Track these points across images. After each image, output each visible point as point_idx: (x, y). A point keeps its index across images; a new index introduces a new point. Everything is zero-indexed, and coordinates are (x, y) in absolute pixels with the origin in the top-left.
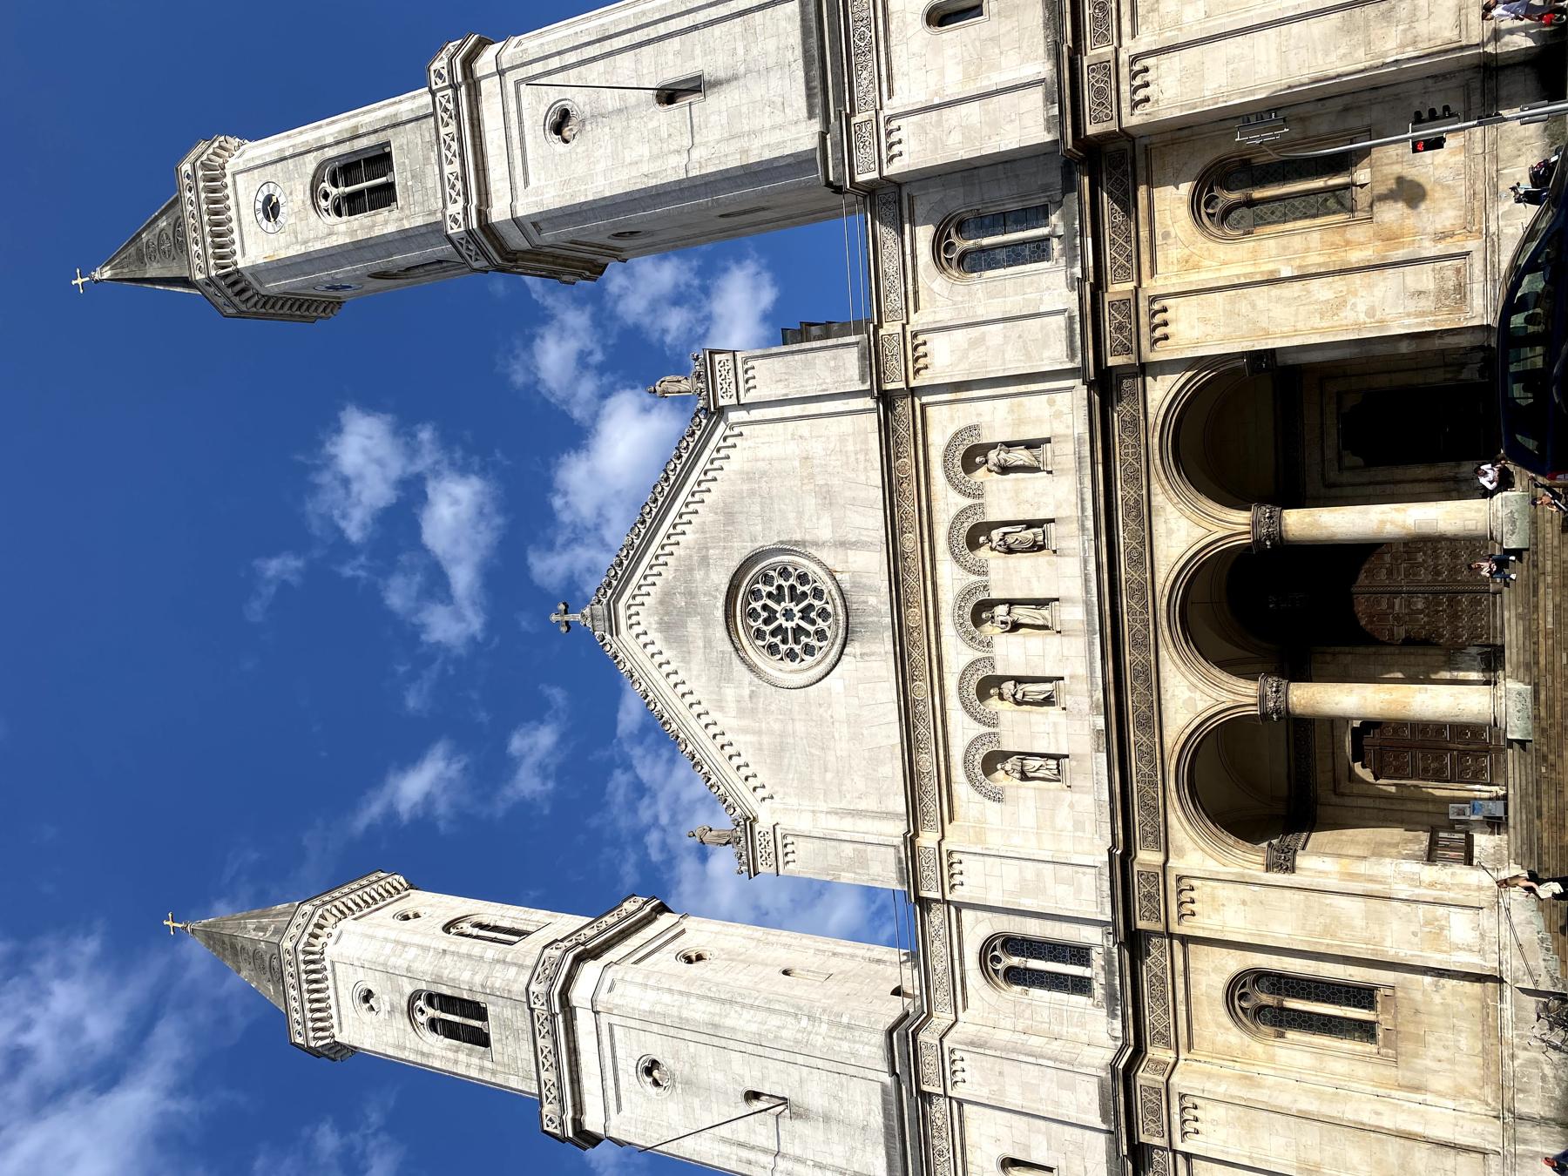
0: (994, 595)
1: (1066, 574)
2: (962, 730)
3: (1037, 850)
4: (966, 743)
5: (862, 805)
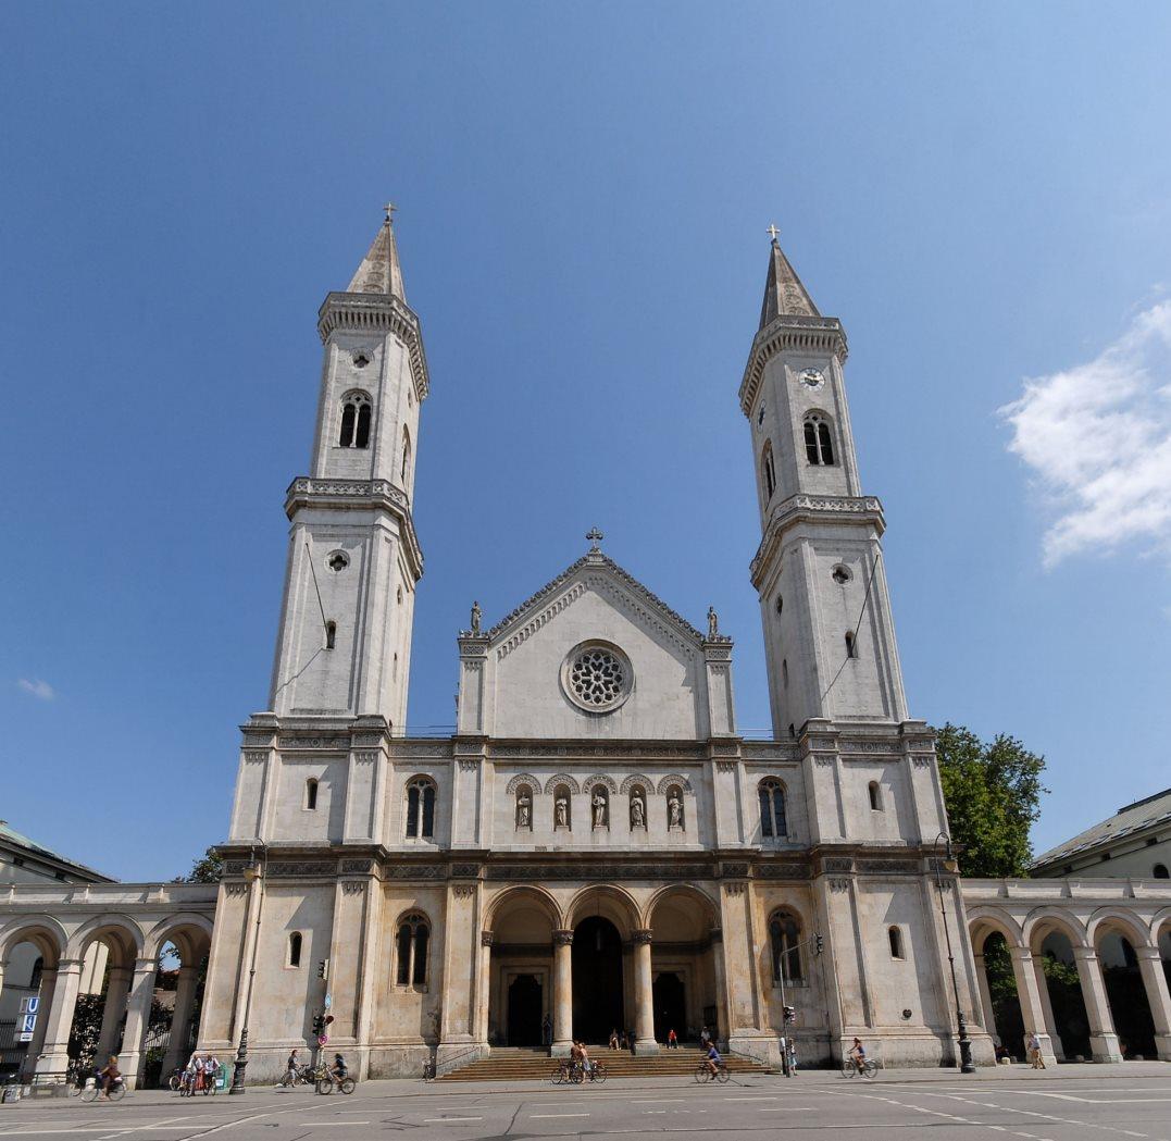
0: (611, 797)
3: (483, 813)
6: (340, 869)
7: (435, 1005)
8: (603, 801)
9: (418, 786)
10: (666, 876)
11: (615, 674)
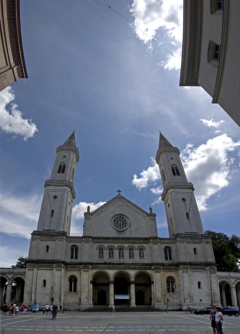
1: (126, 259)
2: (106, 245)
4: (104, 246)
5: (95, 231)
6: (54, 266)
7: (79, 296)
8: (122, 251)
9: (74, 247)
10: (139, 269)
11: (125, 222)
